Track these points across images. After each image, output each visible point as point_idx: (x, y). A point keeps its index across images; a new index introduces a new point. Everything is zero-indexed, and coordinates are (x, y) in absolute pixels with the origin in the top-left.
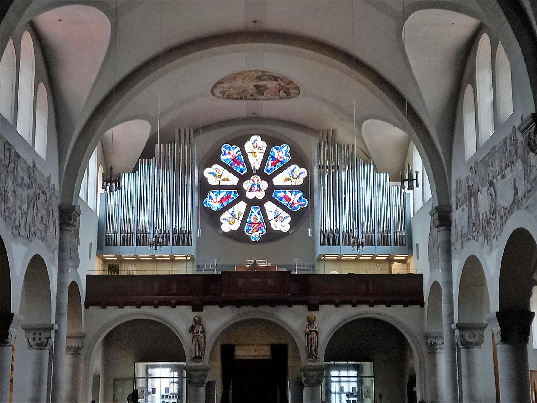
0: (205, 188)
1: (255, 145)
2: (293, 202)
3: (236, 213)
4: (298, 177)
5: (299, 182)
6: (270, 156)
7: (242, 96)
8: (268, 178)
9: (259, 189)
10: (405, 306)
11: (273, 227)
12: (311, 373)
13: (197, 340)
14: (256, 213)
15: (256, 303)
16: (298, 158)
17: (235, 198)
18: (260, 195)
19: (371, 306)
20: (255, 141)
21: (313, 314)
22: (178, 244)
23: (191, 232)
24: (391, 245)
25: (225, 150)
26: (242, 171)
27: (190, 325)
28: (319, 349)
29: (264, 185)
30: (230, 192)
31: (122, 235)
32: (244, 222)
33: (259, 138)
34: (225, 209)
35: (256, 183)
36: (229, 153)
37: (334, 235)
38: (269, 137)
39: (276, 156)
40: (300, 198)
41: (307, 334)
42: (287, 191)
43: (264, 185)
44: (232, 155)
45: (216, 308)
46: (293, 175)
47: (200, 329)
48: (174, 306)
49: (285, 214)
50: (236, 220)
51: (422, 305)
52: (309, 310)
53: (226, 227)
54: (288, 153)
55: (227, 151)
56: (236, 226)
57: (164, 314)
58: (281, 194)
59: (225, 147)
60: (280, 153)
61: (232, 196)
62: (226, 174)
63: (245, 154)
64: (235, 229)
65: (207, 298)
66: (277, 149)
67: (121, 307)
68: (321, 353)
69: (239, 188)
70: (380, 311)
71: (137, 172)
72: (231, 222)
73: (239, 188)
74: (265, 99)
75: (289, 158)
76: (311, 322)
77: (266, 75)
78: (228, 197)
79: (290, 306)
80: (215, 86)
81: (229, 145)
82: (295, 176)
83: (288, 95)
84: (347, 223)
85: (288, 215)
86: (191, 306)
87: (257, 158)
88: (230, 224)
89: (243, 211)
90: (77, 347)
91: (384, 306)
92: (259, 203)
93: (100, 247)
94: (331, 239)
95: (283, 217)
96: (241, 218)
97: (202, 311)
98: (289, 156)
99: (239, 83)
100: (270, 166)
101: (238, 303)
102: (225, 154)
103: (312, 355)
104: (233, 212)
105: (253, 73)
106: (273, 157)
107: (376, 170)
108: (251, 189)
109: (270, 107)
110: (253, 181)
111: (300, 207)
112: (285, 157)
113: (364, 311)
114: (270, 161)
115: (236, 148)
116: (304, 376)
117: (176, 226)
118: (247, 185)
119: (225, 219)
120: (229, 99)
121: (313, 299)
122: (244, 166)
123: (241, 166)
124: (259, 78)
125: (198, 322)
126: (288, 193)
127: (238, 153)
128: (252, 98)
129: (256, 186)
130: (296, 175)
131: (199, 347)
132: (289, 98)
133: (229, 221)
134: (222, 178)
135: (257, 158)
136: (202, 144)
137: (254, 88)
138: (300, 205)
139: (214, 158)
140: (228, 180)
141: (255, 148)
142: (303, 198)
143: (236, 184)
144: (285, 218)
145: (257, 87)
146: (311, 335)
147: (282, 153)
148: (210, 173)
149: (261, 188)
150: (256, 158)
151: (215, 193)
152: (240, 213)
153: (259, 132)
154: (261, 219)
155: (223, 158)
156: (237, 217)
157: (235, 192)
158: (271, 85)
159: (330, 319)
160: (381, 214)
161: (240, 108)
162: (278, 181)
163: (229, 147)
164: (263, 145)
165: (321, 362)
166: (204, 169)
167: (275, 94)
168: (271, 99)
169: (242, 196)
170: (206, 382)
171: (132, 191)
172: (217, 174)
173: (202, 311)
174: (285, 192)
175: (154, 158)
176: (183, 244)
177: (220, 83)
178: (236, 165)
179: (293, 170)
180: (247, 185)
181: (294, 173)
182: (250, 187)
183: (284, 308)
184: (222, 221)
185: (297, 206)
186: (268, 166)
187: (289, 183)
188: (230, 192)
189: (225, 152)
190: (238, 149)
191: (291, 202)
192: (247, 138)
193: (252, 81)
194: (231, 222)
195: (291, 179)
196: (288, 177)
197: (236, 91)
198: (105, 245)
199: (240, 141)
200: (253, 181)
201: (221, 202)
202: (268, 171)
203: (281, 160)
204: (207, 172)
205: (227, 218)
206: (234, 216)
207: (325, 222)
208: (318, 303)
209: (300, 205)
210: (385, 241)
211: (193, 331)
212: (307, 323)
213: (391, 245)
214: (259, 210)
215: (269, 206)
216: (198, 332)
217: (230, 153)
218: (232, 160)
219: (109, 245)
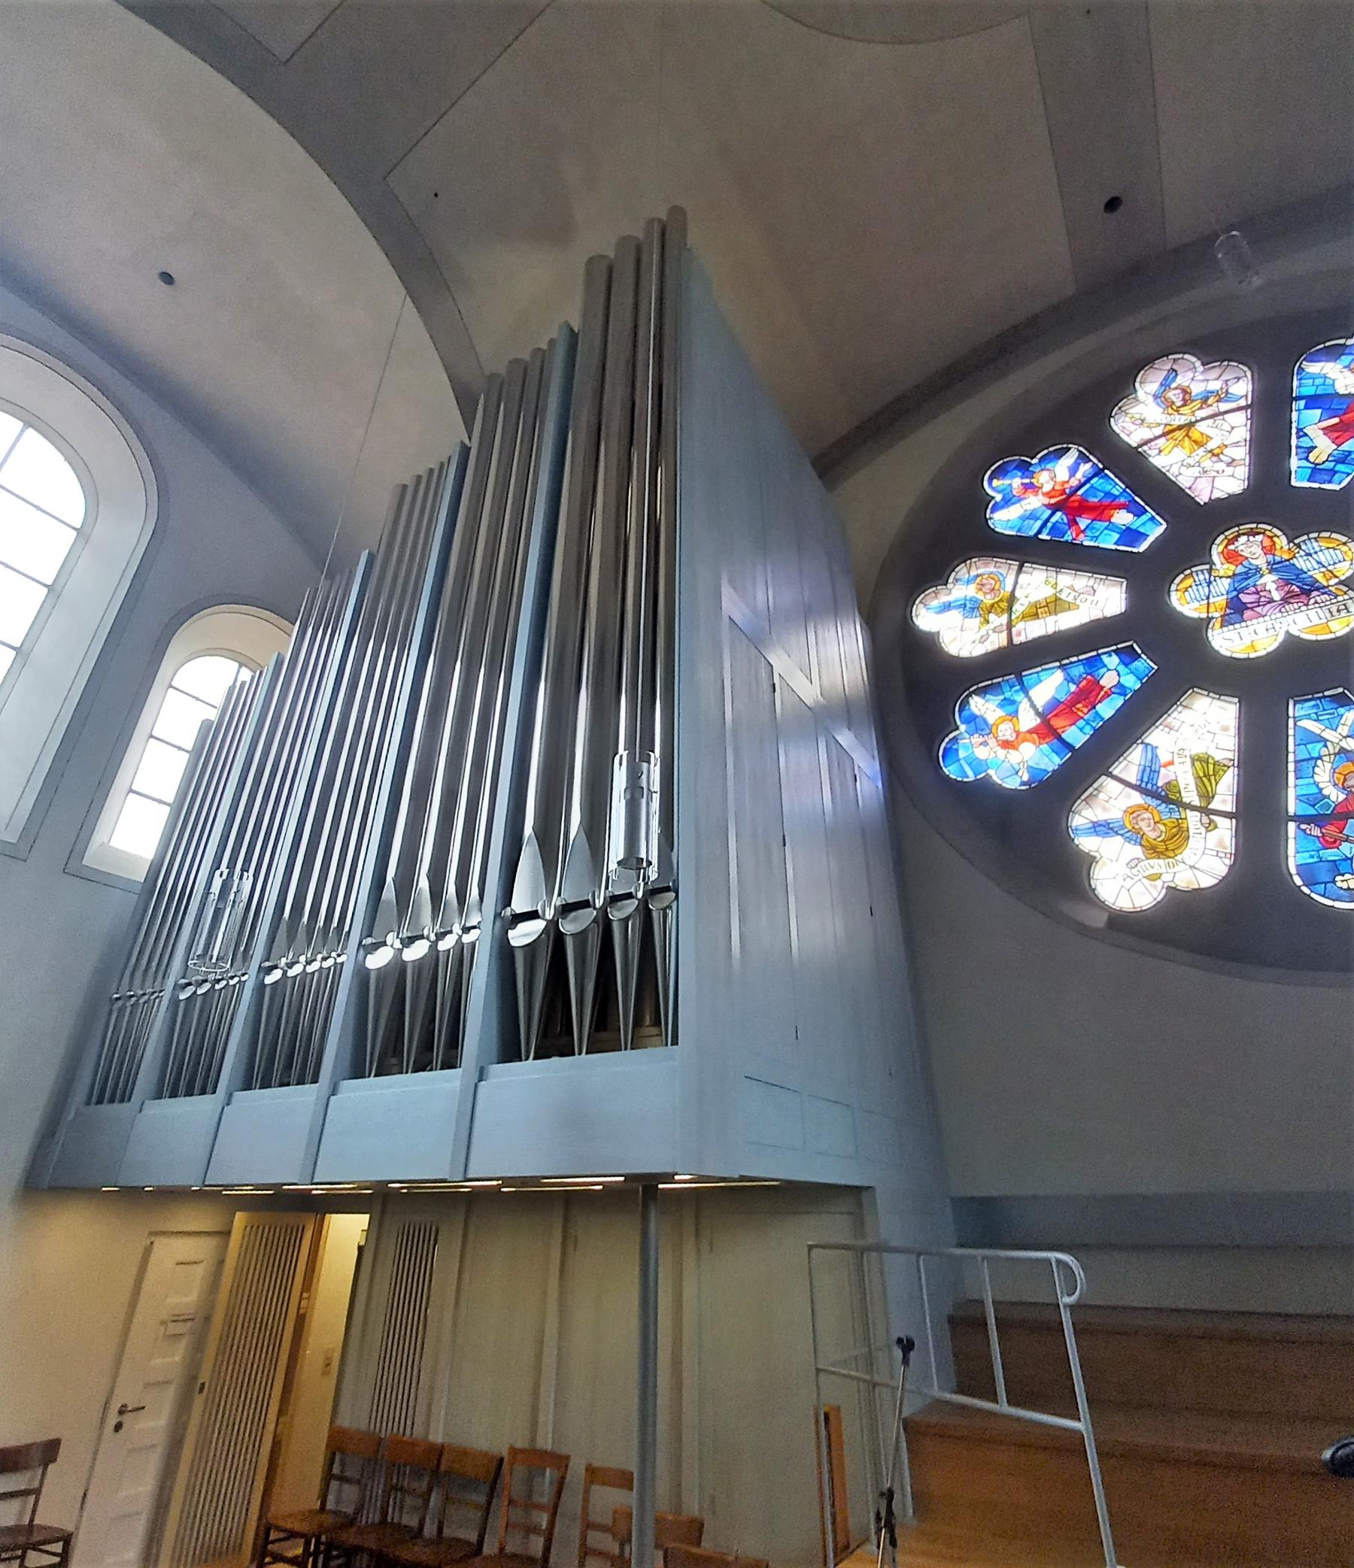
17: (1132, 683)
26: (1131, 535)
30: (1094, 663)
32: (1259, 814)
35: (1261, 562)
44: (1047, 488)
53: (1124, 879)
56: (1206, 860)
61: (1108, 680)
62: (1035, 583)
64: (1207, 882)
78: (1089, 693)
87: (1211, 445)
88: (1154, 851)
100: (1324, 447)
102: (1007, 502)
104: (1150, 770)
122: (1139, 512)
123: (1122, 518)
129: (1269, 581)
133: (1136, 836)
134: (1018, 608)
140: (1055, 605)
150: (1201, 451)
152: (1207, 770)
155: (1004, 520)
156: (1191, 796)
157: (1128, 656)
172: (988, 600)
178: (1083, 522)
182: (1221, 601)
184: (1086, 843)
200: (1231, 557)
201: (1047, 731)
206: (1167, 796)
218: (1054, 508)
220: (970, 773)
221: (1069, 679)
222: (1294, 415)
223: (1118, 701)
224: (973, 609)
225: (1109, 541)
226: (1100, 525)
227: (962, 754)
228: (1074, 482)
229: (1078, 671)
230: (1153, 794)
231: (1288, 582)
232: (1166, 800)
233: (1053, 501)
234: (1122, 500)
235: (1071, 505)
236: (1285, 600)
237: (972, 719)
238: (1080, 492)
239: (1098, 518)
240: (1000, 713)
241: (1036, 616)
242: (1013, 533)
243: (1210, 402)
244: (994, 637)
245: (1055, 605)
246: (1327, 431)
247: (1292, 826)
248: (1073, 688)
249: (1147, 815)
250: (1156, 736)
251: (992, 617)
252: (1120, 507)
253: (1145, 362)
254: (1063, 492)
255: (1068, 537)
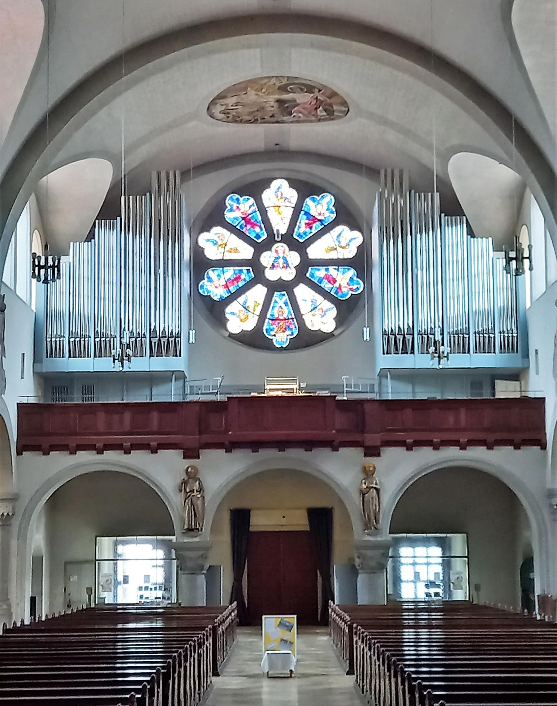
0: (200, 265)
1: (279, 194)
2: (340, 286)
3: (250, 304)
4: (348, 245)
5: (350, 253)
6: (302, 213)
7: (256, 118)
8: (300, 247)
9: (286, 265)
10: (517, 447)
11: (309, 325)
12: (369, 553)
13: (192, 504)
14: (281, 303)
15: (282, 445)
16: (346, 215)
18: (289, 275)
19: (463, 448)
20: (278, 189)
21: (372, 461)
22: (160, 354)
23: (179, 335)
24: (494, 352)
25: (232, 203)
26: (258, 236)
27: (179, 481)
28: (381, 515)
29: (294, 258)
31: (72, 340)
33: (284, 184)
34: (233, 297)
36: (238, 207)
37: (404, 338)
38: (301, 181)
39: (313, 212)
40: (351, 279)
41: (363, 494)
42: (331, 268)
43: (294, 258)
44: (242, 210)
45: (221, 452)
46: (339, 242)
47: (196, 486)
48: (154, 451)
49: (327, 304)
50: (250, 315)
51: (544, 447)
52: (366, 455)
54: (331, 207)
55: (235, 205)
56: (250, 325)
57: (139, 461)
58: (320, 273)
59: (233, 200)
60: (319, 207)
61: (243, 277)
62: (234, 241)
63: (263, 210)
65: (206, 438)
66: (314, 200)
67: (73, 452)
68: (385, 522)
69: (254, 263)
70: (478, 456)
71: (93, 241)
72: (243, 318)
73: (254, 263)
74: (292, 122)
75: (334, 216)
76: (368, 473)
77: (294, 84)
78: (237, 279)
79: (335, 449)
80: (213, 102)
81: (237, 196)
82: (343, 244)
83: (331, 115)
84: (426, 319)
85: (332, 306)
86: (181, 451)
87: (282, 216)
88: (241, 320)
89: (261, 301)
90: (5, 514)
91: (484, 448)
92: (286, 287)
93: (36, 359)
94: (399, 343)
95: (324, 310)
96: (258, 312)
97: (198, 457)
98: (332, 213)
99: (252, 96)
100: (303, 228)
101: (255, 445)
102: (231, 210)
103: (370, 522)
104: (245, 302)
105: (274, 80)
106: (306, 213)
107: (471, 233)
108: (273, 266)
109: (303, 133)
110: (276, 251)
111: (351, 292)
112: (327, 214)
113: (451, 455)
114: (303, 220)
115: (248, 199)
116: (359, 557)
117: (155, 327)
118: (266, 259)
119: (233, 313)
120: (236, 122)
121: (372, 439)
122: (261, 230)
123: (257, 229)
124: (283, 89)
125: (191, 476)
126: (332, 271)
127: (253, 208)
128: (272, 119)
129: (281, 261)
130: (345, 241)
131: (195, 514)
132: (332, 119)
133: (239, 316)
134: (227, 248)
135: (282, 216)
136: (197, 195)
137: (276, 105)
138: (351, 289)
139: (213, 217)
140: (236, 251)
141: (280, 198)
142: (355, 278)
143: (250, 257)
144: (327, 311)
145: (280, 102)
146: (369, 493)
147: (322, 207)
148: (208, 240)
149: (290, 263)
150: (280, 216)
151: (216, 273)
153: (285, 174)
154: (289, 312)
155: (229, 216)
156: (251, 309)
157: (248, 270)
158: (303, 98)
159: (399, 469)
160: (480, 304)
161: (255, 136)
162: (315, 251)
163: (238, 199)
164: (293, 195)
165: (386, 536)
166: (199, 234)
167: (310, 113)
168: (303, 121)
169: (259, 276)
170: (207, 566)
171: (86, 270)
172: (220, 243)
173: (198, 457)
174: (327, 270)
175: (118, 218)
176: (167, 354)
177: (221, 96)
179: (340, 234)
180: (266, 259)
181: (341, 239)
183: (327, 451)
184: (227, 316)
185: (347, 293)
186: (299, 227)
187: (333, 255)
188: (241, 270)
189: (232, 206)
190: (252, 201)
191: (336, 285)
192: (266, 183)
193: (273, 94)
194: (243, 317)
195: (336, 249)
196: (332, 245)
197: (248, 110)
198: (45, 356)
199: (254, 189)
200: (276, 251)
201: (226, 286)
202: (300, 235)
203: (320, 218)
204: (203, 239)
205: (235, 312)
207: (391, 316)
208: (378, 443)
209: (351, 289)
210: (485, 346)
211: (185, 489)
212: (362, 476)
213: (494, 352)
214: (286, 297)
215: (303, 292)
216: (192, 491)
217: (239, 208)
218: (243, 219)
219: (51, 355)
220: (206, 292)
221: (234, 273)
222: (301, 215)
223: (244, 283)
224: (215, 244)
225: (253, 236)
226: (252, 229)
227: (205, 287)
228: (249, 212)
229: (237, 272)
230: (245, 308)
231: (284, 263)
232: (247, 309)
233: (243, 216)
234: (259, 224)
235: (246, 219)
236: (284, 267)
237: (209, 278)
238: (250, 216)
239: (253, 227)
240: (217, 278)
241: (231, 252)
242: (231, 222)
243: (287, 201)
244: (219, 254)
245: (236, 251)
246: (306, 224)
247: (267, 320)
248: (235, 276)
249: (242, 312)
250: (248, 293)
251: (220, 248)
252: (257, 226)
253: (276, 178)
254: (246, 214)
255: (244, 230)
